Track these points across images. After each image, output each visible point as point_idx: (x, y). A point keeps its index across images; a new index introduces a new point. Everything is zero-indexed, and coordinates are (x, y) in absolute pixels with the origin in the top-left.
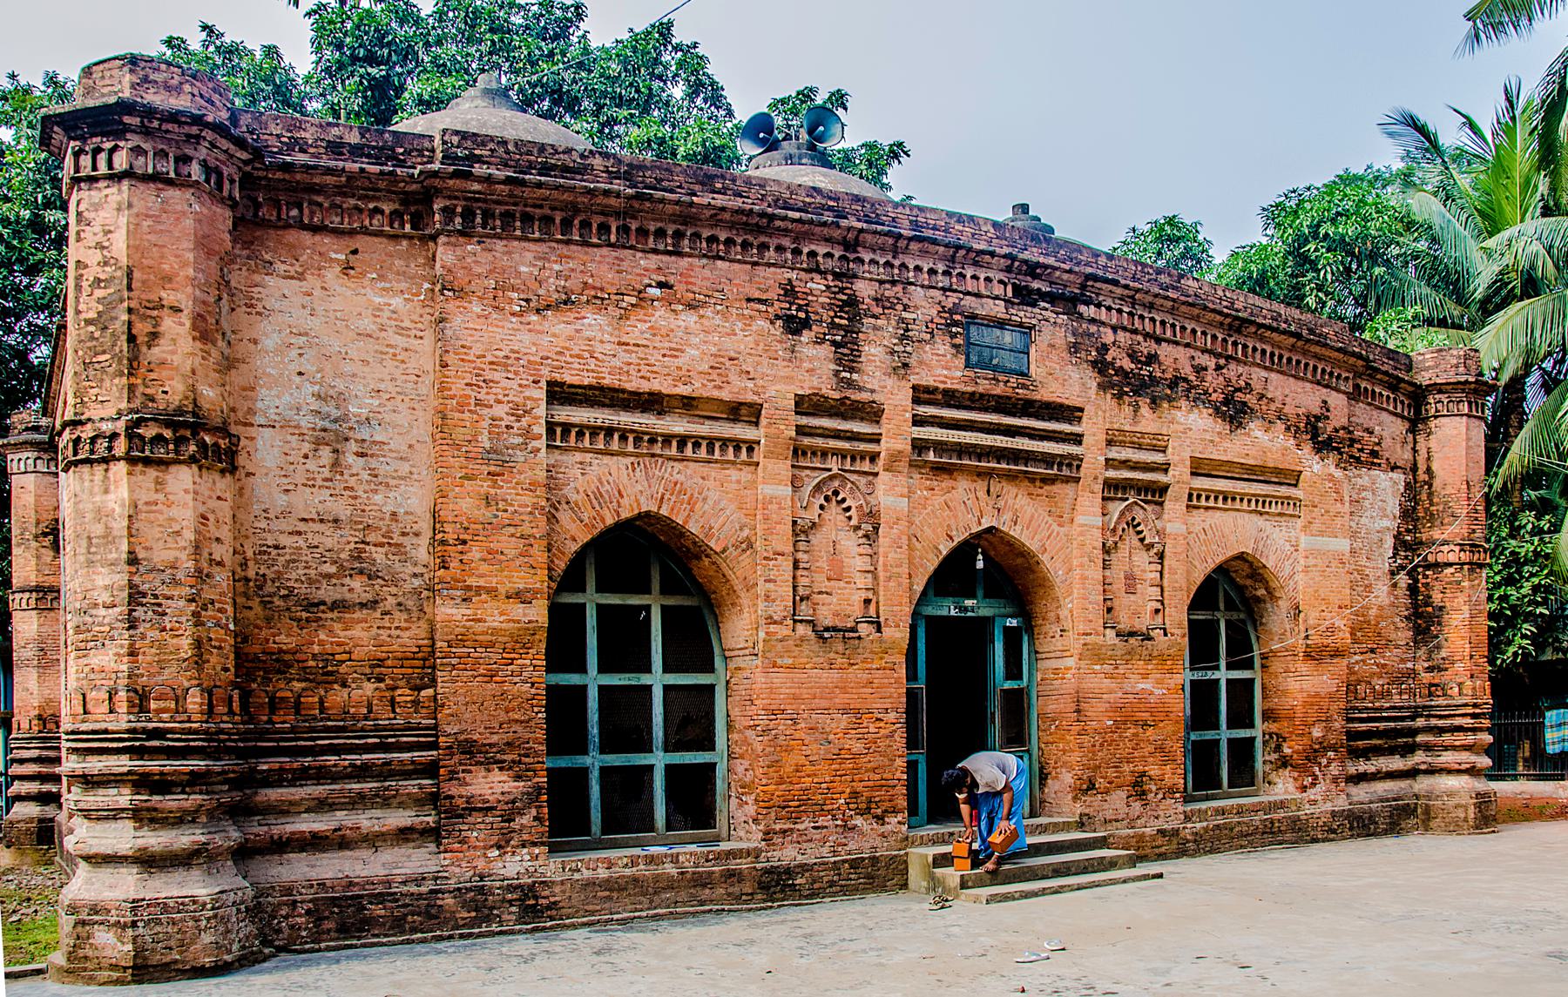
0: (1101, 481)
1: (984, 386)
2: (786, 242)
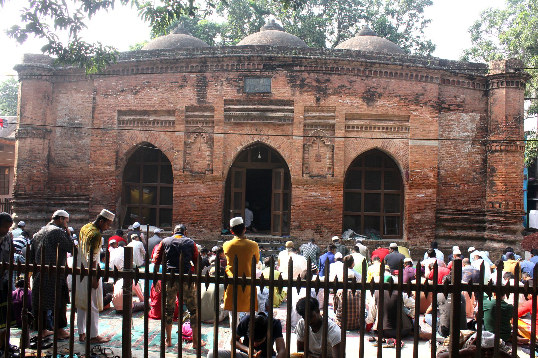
0: (302, 123)
2: (183, 65)
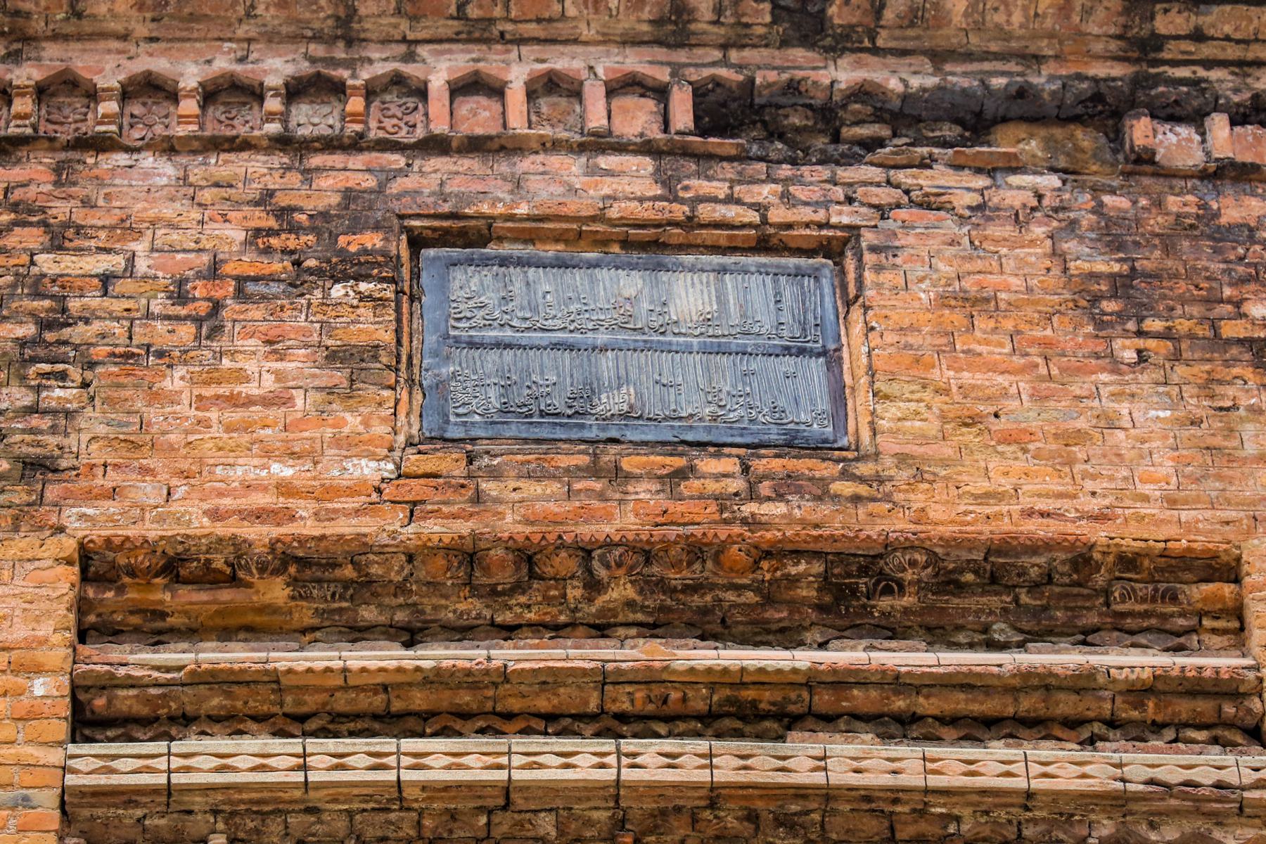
1: (521, 504)
